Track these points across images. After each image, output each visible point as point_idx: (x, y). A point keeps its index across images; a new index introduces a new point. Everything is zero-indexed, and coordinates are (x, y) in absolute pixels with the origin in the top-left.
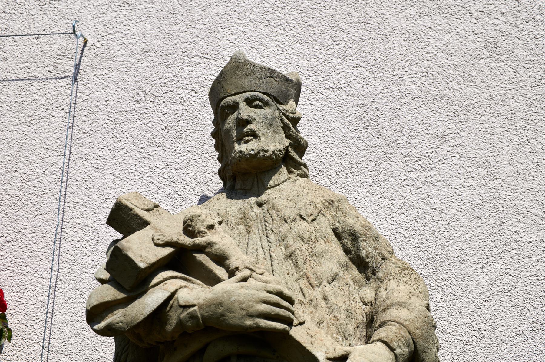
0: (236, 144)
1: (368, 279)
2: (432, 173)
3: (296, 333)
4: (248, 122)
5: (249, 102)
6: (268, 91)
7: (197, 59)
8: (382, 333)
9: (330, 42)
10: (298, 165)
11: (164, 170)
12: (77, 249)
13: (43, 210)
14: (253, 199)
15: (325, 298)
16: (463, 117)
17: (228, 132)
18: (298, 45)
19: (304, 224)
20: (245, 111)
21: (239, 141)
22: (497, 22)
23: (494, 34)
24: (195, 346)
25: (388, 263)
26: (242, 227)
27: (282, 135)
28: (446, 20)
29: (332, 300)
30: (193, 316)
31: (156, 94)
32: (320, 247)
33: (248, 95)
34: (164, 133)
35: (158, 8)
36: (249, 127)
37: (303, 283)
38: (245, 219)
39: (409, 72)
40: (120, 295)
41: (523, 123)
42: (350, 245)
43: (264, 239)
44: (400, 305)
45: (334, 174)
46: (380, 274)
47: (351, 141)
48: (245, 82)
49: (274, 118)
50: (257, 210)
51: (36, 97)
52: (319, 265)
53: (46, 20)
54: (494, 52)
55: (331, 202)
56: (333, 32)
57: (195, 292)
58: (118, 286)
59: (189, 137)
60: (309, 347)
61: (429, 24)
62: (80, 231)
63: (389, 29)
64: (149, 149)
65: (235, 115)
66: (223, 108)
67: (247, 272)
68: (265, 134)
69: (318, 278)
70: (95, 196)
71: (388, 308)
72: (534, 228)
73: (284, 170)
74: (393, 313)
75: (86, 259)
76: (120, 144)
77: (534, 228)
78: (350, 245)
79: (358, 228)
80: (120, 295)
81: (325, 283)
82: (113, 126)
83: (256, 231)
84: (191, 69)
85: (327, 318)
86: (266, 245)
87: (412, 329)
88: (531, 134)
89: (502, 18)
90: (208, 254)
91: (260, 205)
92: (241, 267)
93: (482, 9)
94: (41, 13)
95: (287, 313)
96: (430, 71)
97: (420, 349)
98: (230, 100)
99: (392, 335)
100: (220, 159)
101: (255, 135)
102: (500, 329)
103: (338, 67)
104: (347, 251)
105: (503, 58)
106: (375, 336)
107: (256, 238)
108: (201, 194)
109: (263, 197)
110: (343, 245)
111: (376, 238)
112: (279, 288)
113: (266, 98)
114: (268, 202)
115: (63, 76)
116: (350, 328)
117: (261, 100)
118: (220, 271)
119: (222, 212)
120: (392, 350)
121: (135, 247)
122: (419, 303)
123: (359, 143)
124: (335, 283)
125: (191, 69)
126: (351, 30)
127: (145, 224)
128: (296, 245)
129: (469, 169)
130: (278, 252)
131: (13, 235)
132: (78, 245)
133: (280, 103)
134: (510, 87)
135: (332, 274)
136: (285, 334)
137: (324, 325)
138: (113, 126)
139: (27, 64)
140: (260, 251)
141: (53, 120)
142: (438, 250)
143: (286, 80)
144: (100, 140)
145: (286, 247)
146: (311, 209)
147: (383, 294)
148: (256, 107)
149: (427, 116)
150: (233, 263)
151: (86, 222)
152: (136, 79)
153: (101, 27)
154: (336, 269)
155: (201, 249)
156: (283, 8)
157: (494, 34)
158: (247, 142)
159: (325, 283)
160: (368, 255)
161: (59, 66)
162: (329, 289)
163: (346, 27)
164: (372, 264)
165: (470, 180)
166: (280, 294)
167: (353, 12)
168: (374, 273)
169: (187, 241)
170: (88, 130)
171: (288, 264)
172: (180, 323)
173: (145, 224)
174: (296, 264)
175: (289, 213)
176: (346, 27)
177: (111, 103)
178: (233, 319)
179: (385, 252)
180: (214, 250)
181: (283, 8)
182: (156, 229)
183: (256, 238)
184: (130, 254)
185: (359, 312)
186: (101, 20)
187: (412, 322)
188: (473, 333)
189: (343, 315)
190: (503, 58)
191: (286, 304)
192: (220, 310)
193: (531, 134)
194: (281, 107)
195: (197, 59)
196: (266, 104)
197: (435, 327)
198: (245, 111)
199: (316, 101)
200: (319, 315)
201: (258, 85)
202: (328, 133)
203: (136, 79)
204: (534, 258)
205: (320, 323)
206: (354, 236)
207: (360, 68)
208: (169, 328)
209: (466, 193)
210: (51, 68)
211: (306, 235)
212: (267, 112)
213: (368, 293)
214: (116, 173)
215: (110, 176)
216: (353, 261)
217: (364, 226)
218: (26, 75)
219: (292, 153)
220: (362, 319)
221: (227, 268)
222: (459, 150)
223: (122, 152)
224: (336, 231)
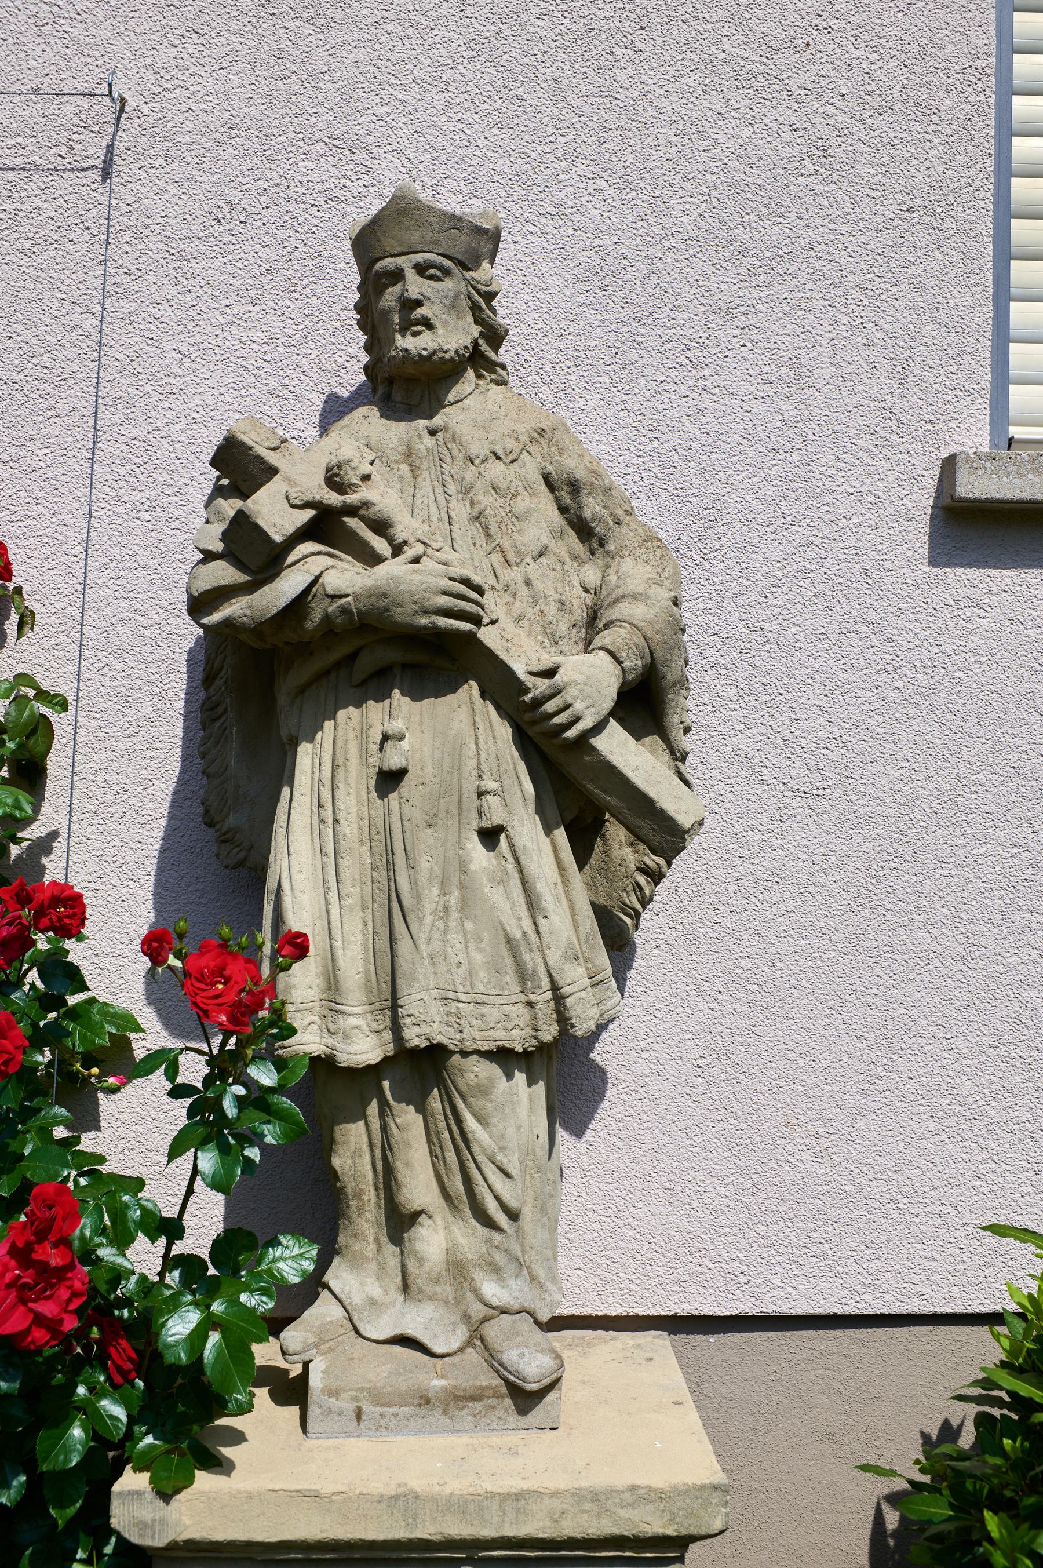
0: (398, 336)
1: (592, 552)
2: (706, 372)
3: (487, 636)
4: (419, 304)
5: (421, 269)
6: (451, 253)
7: (320, 148)
8: (605, 638)
9: (550, 130)
10: (492, 366)
11: (266, 348)
12: (121, 478)
13: (62, 408)
14: (422, 423)
15: (528, 583)
16: (763, 277)
17: (386, 314)
18: (495, 131)
19: (500, 467)
20: (415, 286)
21: (404, 330)
22: (831, 110)
23: (825, 132)
24: (343, 650)
25: (624, 529)
26: (405, 468)
27: (470, 319)
28: (747, 101)
29: (538, 585)
30: (345, 611)
31: (249, 208)
32: (522, 503)
33: (419, 258)
34: (265, 280)
35: (252, 44)
36: (420, 311)
37: (496, 558)
38: (409, 455)
39: (681, 193)
40: (243, 578)
41: (857, 294)
42: (567, 500)
43: (439, 489)
44: (635, 597)
45: (548, 367)
46: (611, 547)
47: (579, 311)
48: (414, 237)
49: (457, 296)
50: (428, 441)
51: (38, 202)
52: (521, 532)
53: (49, 56)
54: (822, 165)
55: (541, 432)
56: (556, 112)
57: (348, 575)
58: (239, 564)
59: (308, 291)
60: (503, 656)
61: (719, 107)
62: (124, 448)
63: (651, 111)
64: (238, 309)
65: (396, 289)
66: (378, 274)
67: (419, 549)
68: (445, 323)
69: (518, 552)
70: (148, 388)
71: (617, 601)
72: (860, 471)
73: (470, 374)
74: (624, 610)
75: (137, 496)
76: (189, 297)
77: (860, 471)
78: (567, 500)
79: (581, 474)
80: (243, 578)
81: (528, 559)
82: (176, 264)
83: (426, 474)
84: (310, 165)
85: (530, 612)
86: (441, 498)
87: (649, 633)
88: (868, 313)
89: (840, 104)
90: (362, 518)
91: (433, 433)
92: (411, 540)
93: (808, 85)
94: (40, 40)
95: (475, 609)
96: (715, 194)
97: (659, 661)
98: (389, 263)
99: (619, 642)
100: (368, 348)
101: (428, 324)
102: (794, 630)
103: (562, 177)
104: (563, 509)
105: (835, 176)
106: (597, 642)
107: (426, 486)
108: (327, 390)
109: (437, 421)
110: (557, 500)
111: (608, 491)
112: (466, 572)
113: (447, 263)
114: (445, 428)
115: (85, 165)
116: (563, 627)
117: (440, 267)
118: (380, 545)
119: (373, 441)
120: (619, 662)
121: (265, 510)
122: (662, 595)
123: (591, 316)
124: (543, 560)
125: (310, 165)
126: (587, 109)
127: (273, 471)
128: (487, 501)
129: (767, 369)
130: (461, 510)
131: (12, 450)
132: (122, 471)
133: (468, 269)
134: (843, 228)
135: (539, 546)
136: (471, 637)
137: (525, 623)
138: (176, 264)
139: (19, 139)
140: (433, 508)
141: (70, 247)
142: (707, 502)
143: (480, 231)
144: (153, 288)
145: (472, 503)
146: (510, 444)
147: (613, 578)
148: (431, 278)
149: (704, 274)
150: (401, 533)
151: (136, 432)
152: (214, 178)
153: (149, 75)
154: (545, 539)
155: (352, 511)
156: (471, 59)
157: (825, 132)
158: (415, 334)
159: (528, 559)
160: (594, 517)
161: (77, 147)
162: (534, 569)
163: (578, 102)
164: (600, 530)
165: (767, 387)
166: (466, 582)
167: (592, 76)
168: (602, 545)
169: (334, 499)
170: (133, 268)
171: (475, 529)
172: (327, 618)
173: (273, 471)
174: (486, 529)
175: (477, 449)
176: (578, 102)
177: (173, 222)
178: (402, 615)
179: (620, 513)
180: (371, 513)
181: (471, 59)
182: (288, 479)
183: (426, 486)
184: (261, 523)
185: (576, 603)
186: (148, 61)
187: (651, 623)
188: (753, 635)
189: (552, 609)
190: (835, 176)
191: (473, 595)
192: (384, 603)
193: (868, 313)
194: (469, 275)
195: (320, 148)
196: (447, 272)
197: (683, 631)
198: (415, 286)
199: (525, 237)
200: (518, 607)
201: (436, 242)
202: (540, 295)
203: (214, 178)
204: (855, 520)
205: (519, 619)
206: (574, 487)
207: (598, 181)
208: (309, 625)
209: (758, 408)
210: (64, 150)
211: (503, 486)
212: (448, 285)
213: (591, 575)
214: (183, 349)
215: (174, 353)
216: (571, 524)
217: (591, 471)
218: (18, 161)
219: (484, 347)
220: (580, 614)
221: (391, 541)
222: (753, 334)
223: (192, 312)
224: (547, 478)
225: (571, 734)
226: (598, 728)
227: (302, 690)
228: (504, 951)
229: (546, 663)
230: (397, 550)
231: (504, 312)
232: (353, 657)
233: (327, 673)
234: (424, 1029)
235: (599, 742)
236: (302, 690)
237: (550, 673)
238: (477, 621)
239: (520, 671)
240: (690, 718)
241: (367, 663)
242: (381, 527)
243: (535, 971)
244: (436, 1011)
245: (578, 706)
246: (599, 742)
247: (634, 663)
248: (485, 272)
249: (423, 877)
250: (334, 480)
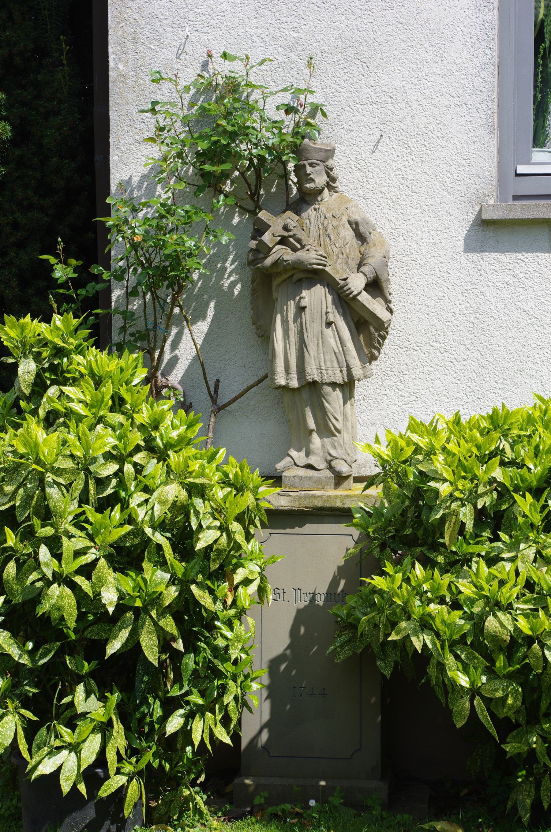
3: (327, 269)
24: (289, 274)
33: (310, 161)
106: (362, 269)
117: (316, 164)
120: (366, 276)
136: (324, 270)
143: (328, 151)
155: (290, 236)
166: (321, 256)
169: (286, 234)
191: (323, 259)
206: (357, 223)
225: (351, 296)
226: (359, 293)
227: (279, 285)
228: (334, 355)
229: (344, 277)
230: (303, 247)
231: (335, 173)
232: (292, 276)
233: (285, 280)
234: (312, 377)
235: (359, 298)
236: (279, 285)
237: (345, 279)
238: (325, 266)
239: (338, 280)
240: (391, 291)
241: (295, 278)
242: (299, 241)
243: (342, 362)
244: (315, 371)
245: (352, 289)
246: (359, 298)
247: (371, 276)
248: (330, 163)
249: (309, 335)
250: (286, 228)
